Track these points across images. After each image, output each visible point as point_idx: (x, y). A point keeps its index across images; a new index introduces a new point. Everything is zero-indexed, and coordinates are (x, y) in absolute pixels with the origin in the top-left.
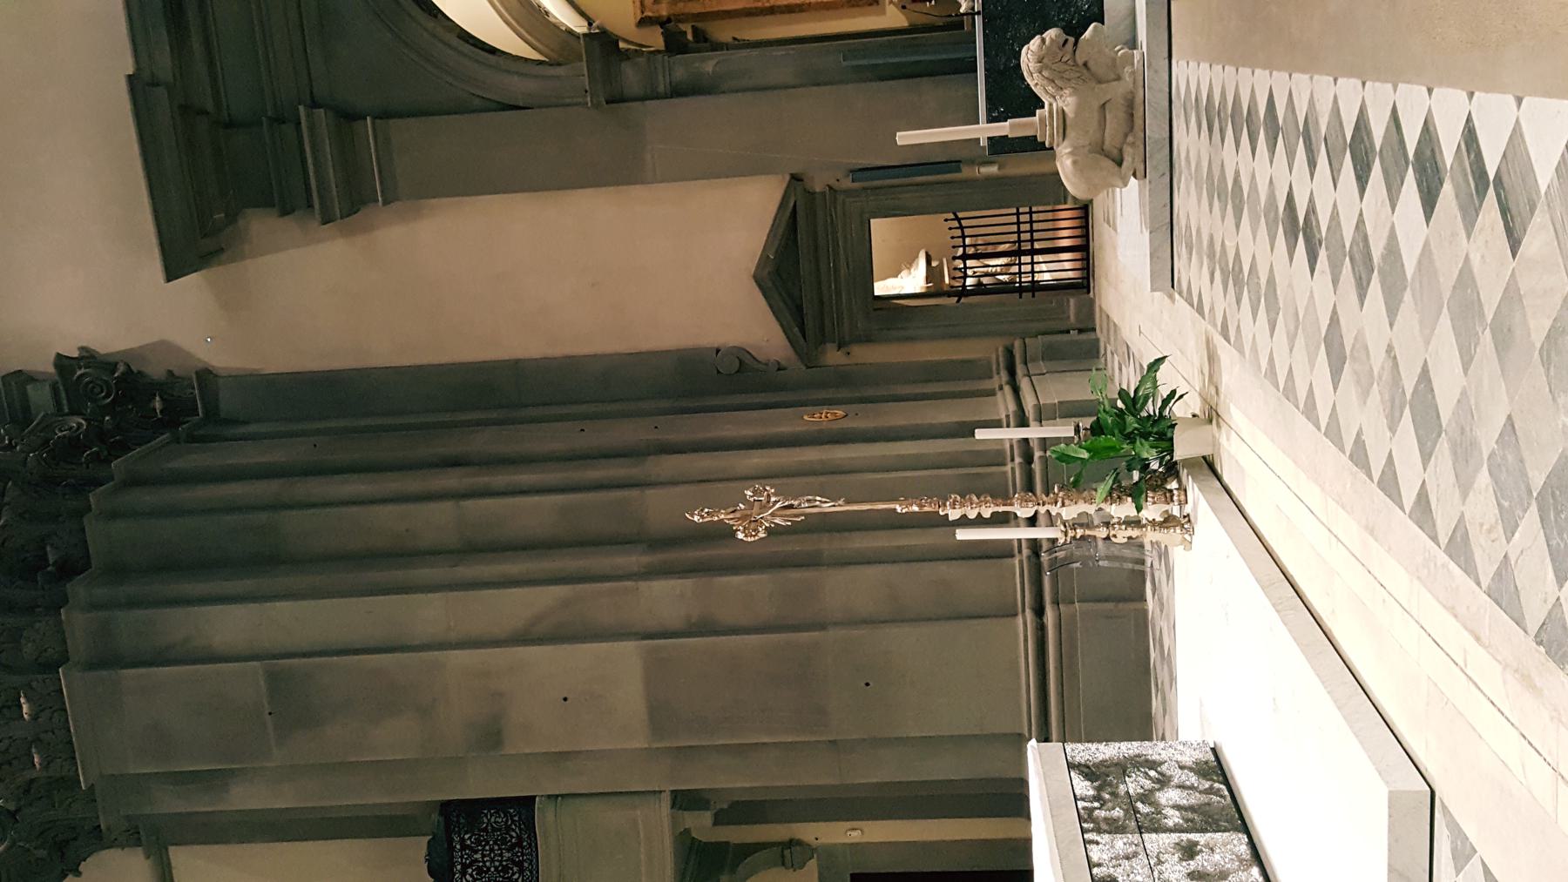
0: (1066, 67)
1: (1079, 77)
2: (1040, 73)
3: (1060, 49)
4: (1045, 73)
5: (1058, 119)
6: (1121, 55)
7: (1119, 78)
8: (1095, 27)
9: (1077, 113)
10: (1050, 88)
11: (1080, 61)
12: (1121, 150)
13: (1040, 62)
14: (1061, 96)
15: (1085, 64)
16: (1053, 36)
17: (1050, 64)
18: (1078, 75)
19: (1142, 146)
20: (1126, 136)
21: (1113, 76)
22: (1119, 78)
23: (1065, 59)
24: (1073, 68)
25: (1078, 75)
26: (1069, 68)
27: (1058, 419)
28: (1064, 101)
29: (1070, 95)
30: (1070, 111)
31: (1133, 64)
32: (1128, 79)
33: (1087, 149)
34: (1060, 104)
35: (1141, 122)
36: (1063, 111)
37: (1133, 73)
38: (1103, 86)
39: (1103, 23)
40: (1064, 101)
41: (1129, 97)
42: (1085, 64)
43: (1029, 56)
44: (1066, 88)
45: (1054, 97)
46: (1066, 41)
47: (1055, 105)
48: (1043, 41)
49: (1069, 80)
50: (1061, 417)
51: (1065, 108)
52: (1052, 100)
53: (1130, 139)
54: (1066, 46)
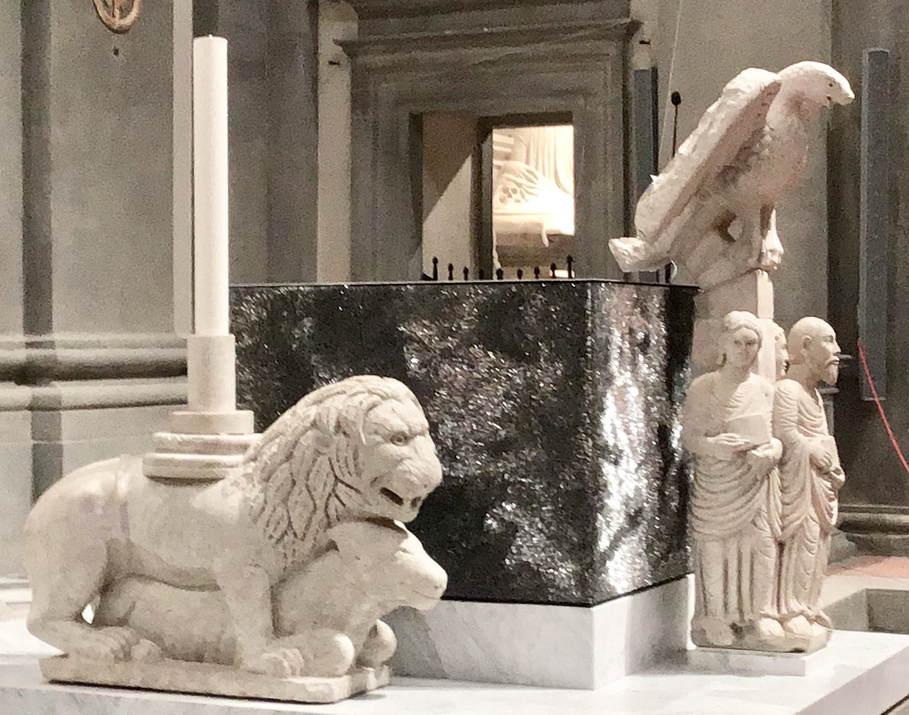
0: (321, 494)
1: (290, 524)
2: (314, 425)
3: (375, 480)
4: (308, 440)
5: (190, 463)
6: (336, 647)
7: (278, 629)
8: (427, 580)
9: (202, 514)
10: (274, 449)
11: (335, 533)
12: (122, 622)
13: (338, 426)
14: (248, 477)
15: (332, 546)
16: (407, 465)
17: (331, 451)
18: (298, 527)
19: (109, 680)
20: (157, 638)
21: (289, 615)
22: (278, 629)
23: (341, 489)
24: (320, 513)
25: (298, 527)
26: (320, 503)
27: (32, 442)
28: (236, 484)
29: (246, 500)
30: (209, 497)
31: (305, 673)
32: (266, 656)
33: (117, 534)
34: (233, 475)
36: (213, 480)
37: (278, 671)
38: (260, 590)
39: (444, 598)
40: (236, 484)
41: (236, 659)
42: (332, 546)
43: (360, 397)
44: (264, 490)
45: (254, 459)
46: (396, 499)
47: (238, 458)
48: (401, 438)
49: (285, 501)
50: (35, 447)
51: (220, 484)
52: (251, 452)
53: (145, 647)
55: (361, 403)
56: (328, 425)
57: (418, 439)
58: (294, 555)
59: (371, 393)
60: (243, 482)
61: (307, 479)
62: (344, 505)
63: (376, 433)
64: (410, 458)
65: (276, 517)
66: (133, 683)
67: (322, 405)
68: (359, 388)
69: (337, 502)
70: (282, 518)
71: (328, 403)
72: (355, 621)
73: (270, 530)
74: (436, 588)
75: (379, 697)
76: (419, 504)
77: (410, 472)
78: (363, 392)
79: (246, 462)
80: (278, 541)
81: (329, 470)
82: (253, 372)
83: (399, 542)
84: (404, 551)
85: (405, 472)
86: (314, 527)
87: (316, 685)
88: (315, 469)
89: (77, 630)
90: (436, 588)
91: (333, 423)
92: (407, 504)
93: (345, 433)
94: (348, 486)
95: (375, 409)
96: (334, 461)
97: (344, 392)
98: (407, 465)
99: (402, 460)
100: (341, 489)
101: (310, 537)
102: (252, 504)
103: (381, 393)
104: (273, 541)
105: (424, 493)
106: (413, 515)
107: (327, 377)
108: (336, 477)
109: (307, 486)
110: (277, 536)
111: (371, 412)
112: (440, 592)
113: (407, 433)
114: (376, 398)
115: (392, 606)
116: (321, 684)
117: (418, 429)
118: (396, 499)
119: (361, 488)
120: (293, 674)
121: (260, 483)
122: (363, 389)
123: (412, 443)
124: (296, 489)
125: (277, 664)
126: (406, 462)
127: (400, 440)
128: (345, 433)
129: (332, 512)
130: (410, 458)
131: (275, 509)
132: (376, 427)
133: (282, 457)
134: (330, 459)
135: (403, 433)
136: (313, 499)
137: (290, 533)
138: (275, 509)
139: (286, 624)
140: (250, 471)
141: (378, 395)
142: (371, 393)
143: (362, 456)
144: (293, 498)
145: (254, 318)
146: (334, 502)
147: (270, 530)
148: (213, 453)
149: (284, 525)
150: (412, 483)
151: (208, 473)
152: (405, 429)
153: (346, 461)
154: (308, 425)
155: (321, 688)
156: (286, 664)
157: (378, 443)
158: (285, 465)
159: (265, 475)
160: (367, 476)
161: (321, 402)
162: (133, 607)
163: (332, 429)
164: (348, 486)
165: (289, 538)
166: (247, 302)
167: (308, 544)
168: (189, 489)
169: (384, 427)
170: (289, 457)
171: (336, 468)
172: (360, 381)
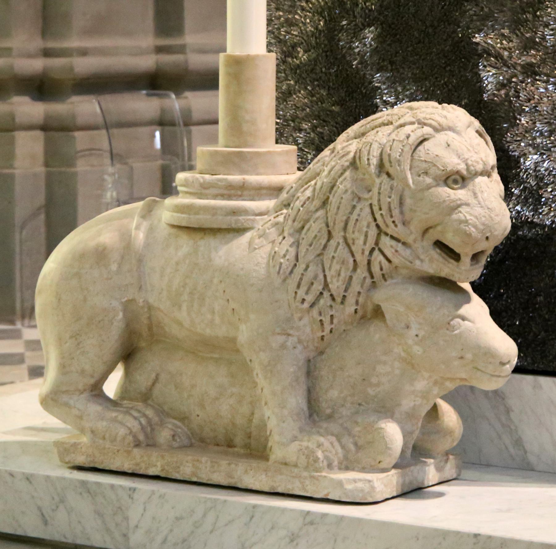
1: (326, 285)
2: (354, 164)
5: (214, 210)
13: (381, 166)
16: (464, 213)
19: (127, 467)
24: (362, 272)
25: (336, 286)
26: (362, 260)
29: (273, 256)
35: (186, 472)
36: (240, 231)
43: (408, 129)
44: (297, 244)
45: (287, 205)
46: (455, 256)
47: (269, 204)
51: (248, 235)
54: (435, 254)
55: (408, 137)
56: (369, 164)
57: (481, 180)
58: (332, 322)
59: (422, 124)
60: (273, 233)
61: (345, 228)
62: (389, 261)
63: (426, 173)
64: (468, 205)
65: (310, 274)
66: (152, 472)
67: (364, 140)
68: (408, 118)
69: (381, 258)
70: (316, 277)
71: (370, 136)
72: (407, 404)
73: (301, 293)
74: (503, 364)
75: (440, 495)
76: (483, 261)
77: (466, 221)
78: (412, 123)
79: (277, 210)
80: (312, 305)
81: (370, 219)
82: (311, 94)
83: (458, 306)
84: (463, 319)
85: (461, 222)
86: (356, 287)
87: (355, 481)
88: (354, 217)
89: (94, 408)
90: (503, 364)
91: (374, 161)
92: (466, 260)
93: (388, 175)
94: (392, 237)
95: (426, 143)
96: (376, 208)
97: (392, 123)
98: (464, 213)
99: (459, 206)
100: (386, 242)
101: (351, 300)
102: (282, 260)
103: (434, 123)
104: (306, 305)
105: (489, 247)
106: (476, 273)
107: (392, 99)
108: (378, 226)
109: (345, 239)
110: (310, 298)
111: (420, 148)
112: (509, 368)
113: (465, 173)
114: (427, 130)
115: (450, 386)
116: (360, 480)
117: (480, 167)
118: (455, 256)
119: (410, 240)
120: (330, 466)
121: (291, 235)
122: (414, 120)
123: (470, 186)
124: (333, 243)
125: (310, 455)
126: (463, 209)
127: (455, 182)
128: (388, 175)
129: (376, 269)
130: (468, 205)
131: (307, 267)
132: (424, 165)
133: (317, 203)
134: (371, 205)
135: (458, 172)
136: (353, 255)
137: (326, 294)
138: (307, 267)
139: (326, 408)
140: (281, 219)
141: (430, 126)
142: (422, 124)
143: (408, 201)
144: (330, 252)
145: (310, 28)
146: (377, 257)
147: (301, 293)
148: (240, 197)
149: (318, 287)
150: (469, 235)
151: (231, 221)
152: (462, 167)
153: (390, 210)
154: (347, 164)
155: (360, 485)
156: (320, 454)
157: (429, 187)
158: (320, 213)
159: (297, 225)
160: (416, 227)
161: (363, 134)
162: (156, 380)
163: (373, 169)
164: (392, 237)
165: (325, 301)
166: (303, 9)
167: (350, 308)
168: (211, 241)
169: (435, 165)
170: (325, 203)
171: (378, 216)
172: (411, 109)
